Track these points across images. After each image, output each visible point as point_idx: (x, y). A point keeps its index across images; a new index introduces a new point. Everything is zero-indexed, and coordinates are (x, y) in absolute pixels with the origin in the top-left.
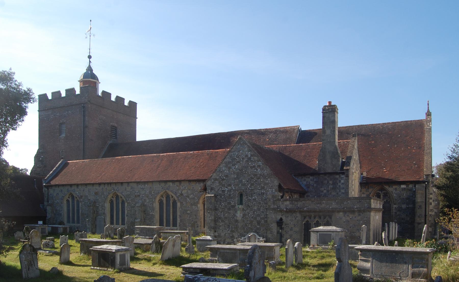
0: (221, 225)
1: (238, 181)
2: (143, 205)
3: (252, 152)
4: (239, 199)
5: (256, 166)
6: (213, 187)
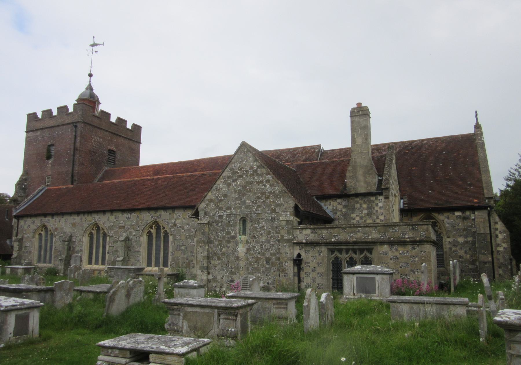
0: (217, 264)
1: (239, 202)
2: (127, 239)
3: (259, 163)
4: (242, 228)
5: (265, 181)
6: (207, 211)
